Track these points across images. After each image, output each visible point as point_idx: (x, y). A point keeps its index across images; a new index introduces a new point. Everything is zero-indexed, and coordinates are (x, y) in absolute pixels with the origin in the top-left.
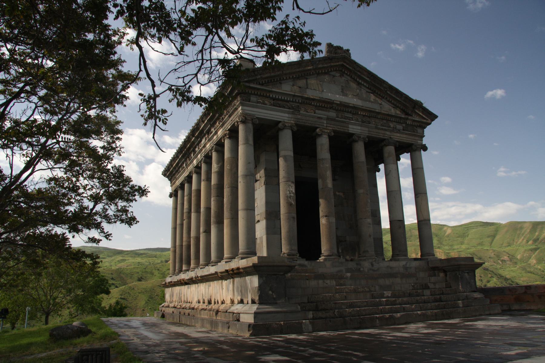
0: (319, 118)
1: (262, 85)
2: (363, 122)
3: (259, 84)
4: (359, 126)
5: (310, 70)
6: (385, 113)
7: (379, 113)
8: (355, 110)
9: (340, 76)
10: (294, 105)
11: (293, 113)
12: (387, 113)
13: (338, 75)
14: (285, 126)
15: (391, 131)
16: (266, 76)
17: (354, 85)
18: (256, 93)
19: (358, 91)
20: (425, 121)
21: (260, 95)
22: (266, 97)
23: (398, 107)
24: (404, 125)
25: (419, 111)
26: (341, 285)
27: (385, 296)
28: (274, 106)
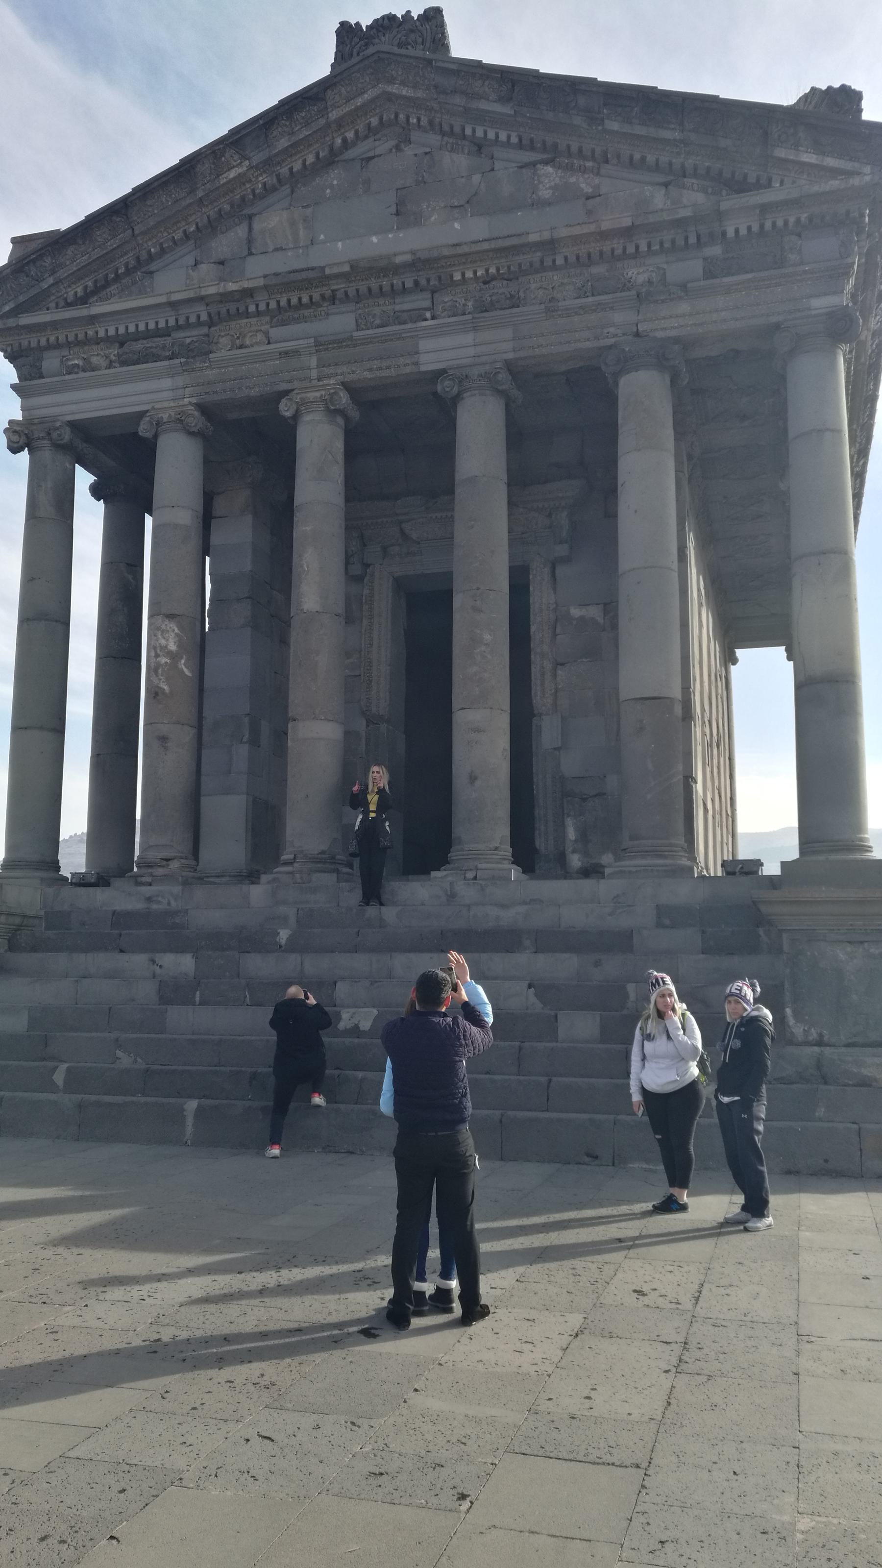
2: (483, 308)
3: (68, 305)
5: (241, 180)
6: (577, 231)
7: (550, 245)
9: (398, 148)
10: (188, 336)
12: (592, 228)
13: (384, 146)
14: (159, 423)
17: (456, 162)
19: (476, 178)
21: (69, 345)
22: (87, 342)
24: (715, 250)
25: (796, 146)
28: (123, 363)
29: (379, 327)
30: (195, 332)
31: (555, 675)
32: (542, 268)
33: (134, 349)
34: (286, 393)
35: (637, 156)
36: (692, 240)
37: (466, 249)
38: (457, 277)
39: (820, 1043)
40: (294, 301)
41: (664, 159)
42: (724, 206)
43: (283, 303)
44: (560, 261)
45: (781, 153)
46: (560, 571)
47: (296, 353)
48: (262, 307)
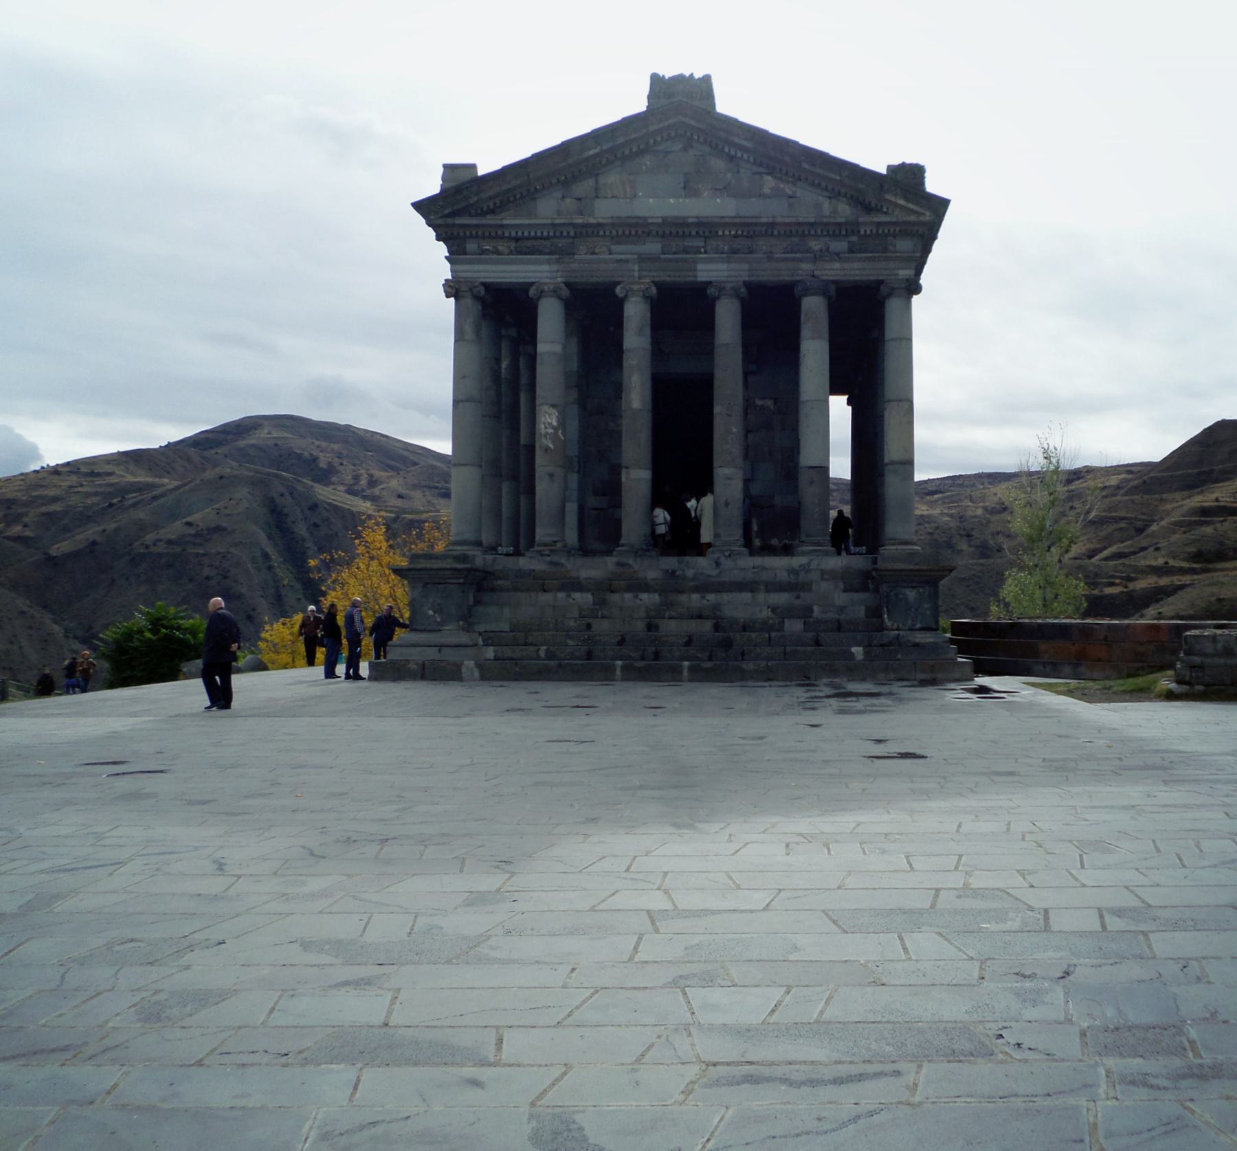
0: (621, 261)
1: (492, 212)
4: (723, 262)
6: (787, 220)
8: (706, 229)
9: (685, 149)
10: (561, 243)
11: (558, 261)
12: (794, 220)
14: (542, 291)
15: (815, 259)
16: (491, 193)
17: (718, 164)
19: (729, 176)
20: (912, 218)
21: (484, 237)
22: (497, 237)
23: (839, 194)
24: (854, 239)
25: (895, 195)
28: (520, 253)
33: (525, 245)
36: (843, 232)
37: (727, 220)
38: (720, 233)
39: (898, 629)
41: (830, 186)
42: (861, 220)
43: (620, 232)
44: (776, 233)
47: (626, 261)
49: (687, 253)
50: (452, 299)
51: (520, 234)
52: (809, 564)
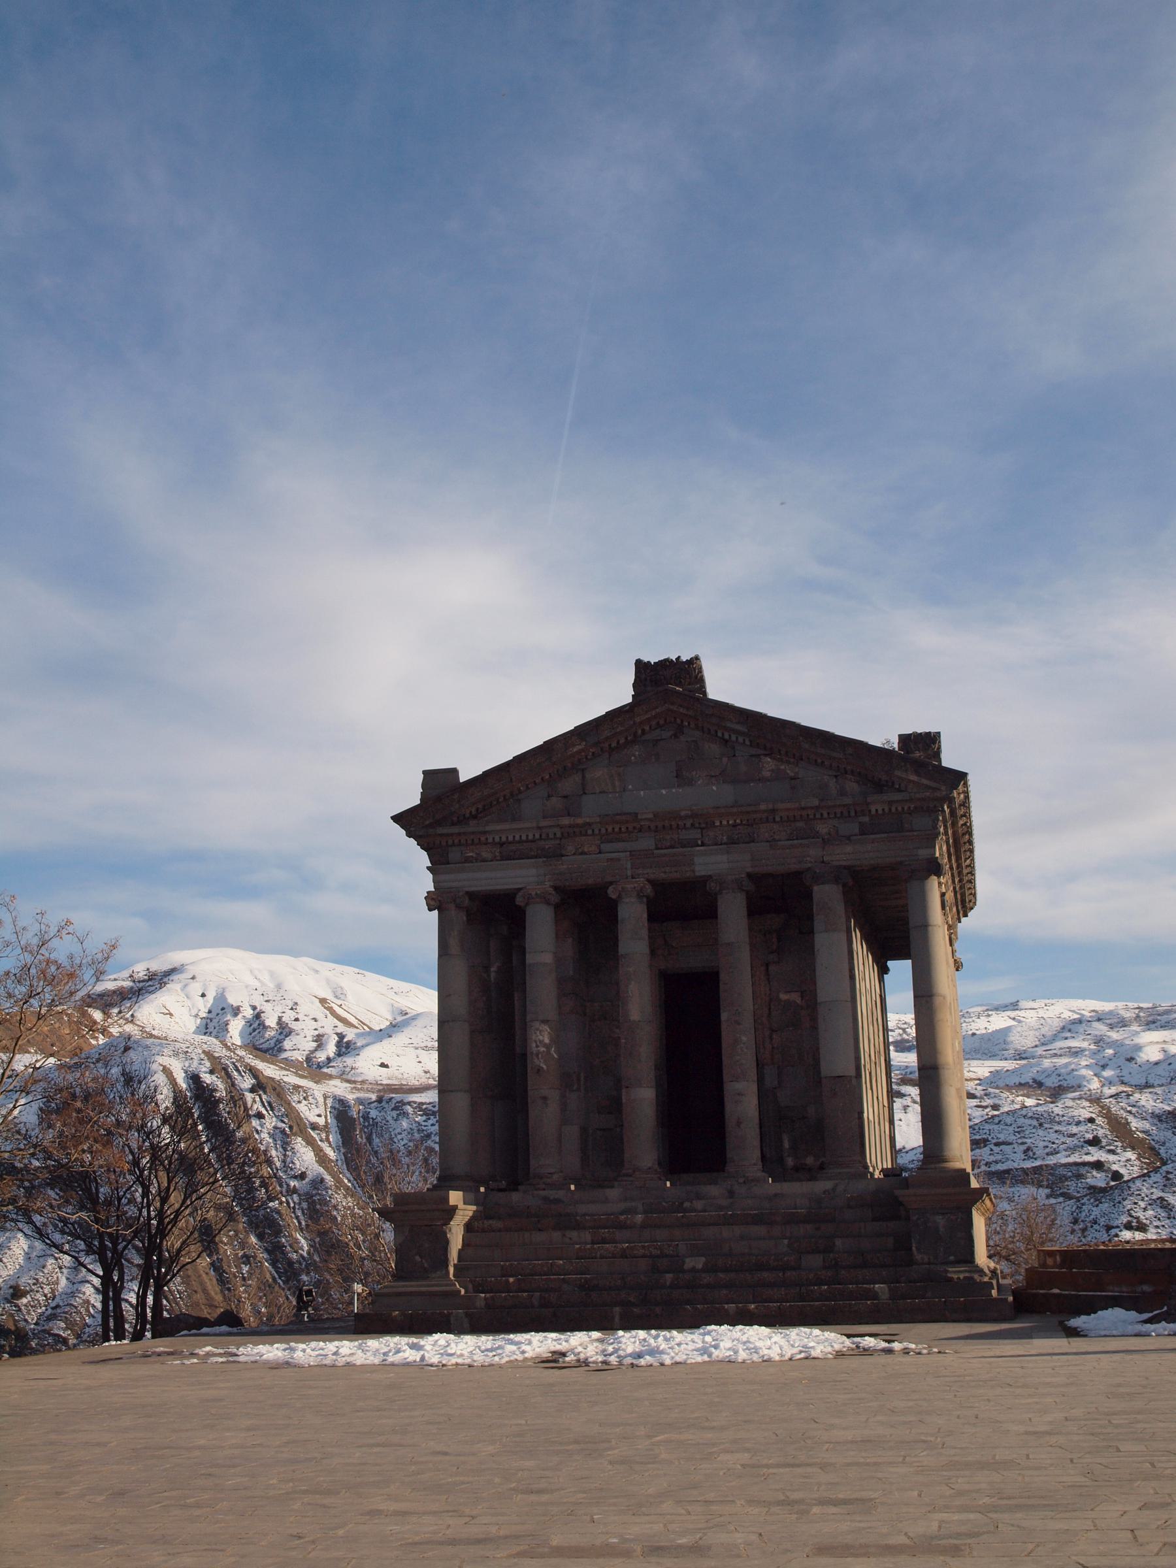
1: (475, 817)
2: (732, 842)
5: (579, 752)
6: (789, 805)
7: (773, 811)
9: (676, 736)
18: (456, 841)
19: (725, 760)
22: (480, 843)
24: (866, 819)
26: (604, 1241)
27: (686, 1267)
29: (672, 847)
30: (553, 842)
31: (771, 1038)
32: (767, 821)
34: (611, 883)
35: (819, 761)
36: (853, 814)
37: (723, 810)
38: (717, 823)
40: (617, 830)
42: (869, 800)
43: (610, 830)
44: (777, 819)
45: (898, 773)
46: (772, 968)
48: (597, 832)
49: (683, 846)
50: (436, 912)
51: (504, 839)
52: (834, 1189)
